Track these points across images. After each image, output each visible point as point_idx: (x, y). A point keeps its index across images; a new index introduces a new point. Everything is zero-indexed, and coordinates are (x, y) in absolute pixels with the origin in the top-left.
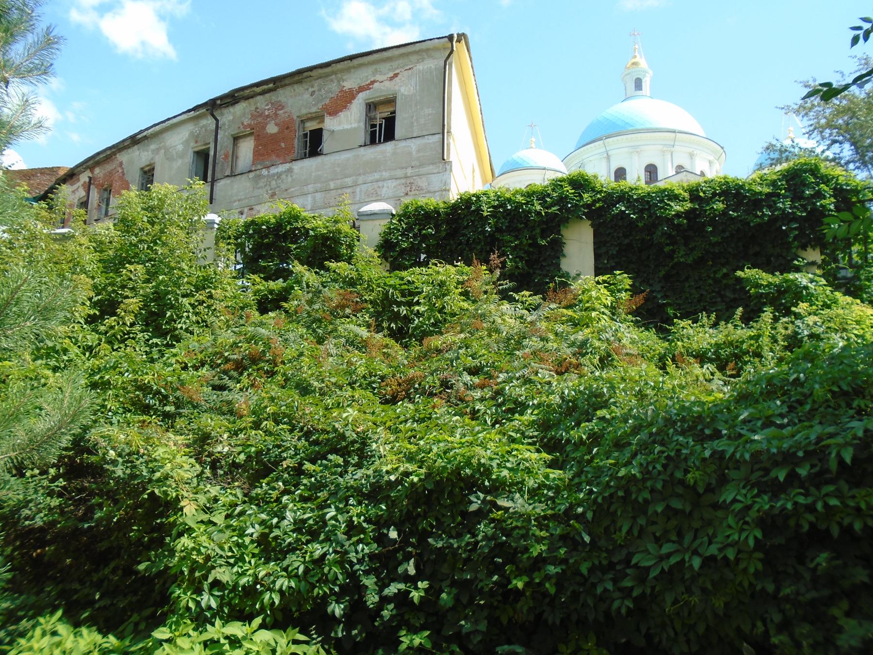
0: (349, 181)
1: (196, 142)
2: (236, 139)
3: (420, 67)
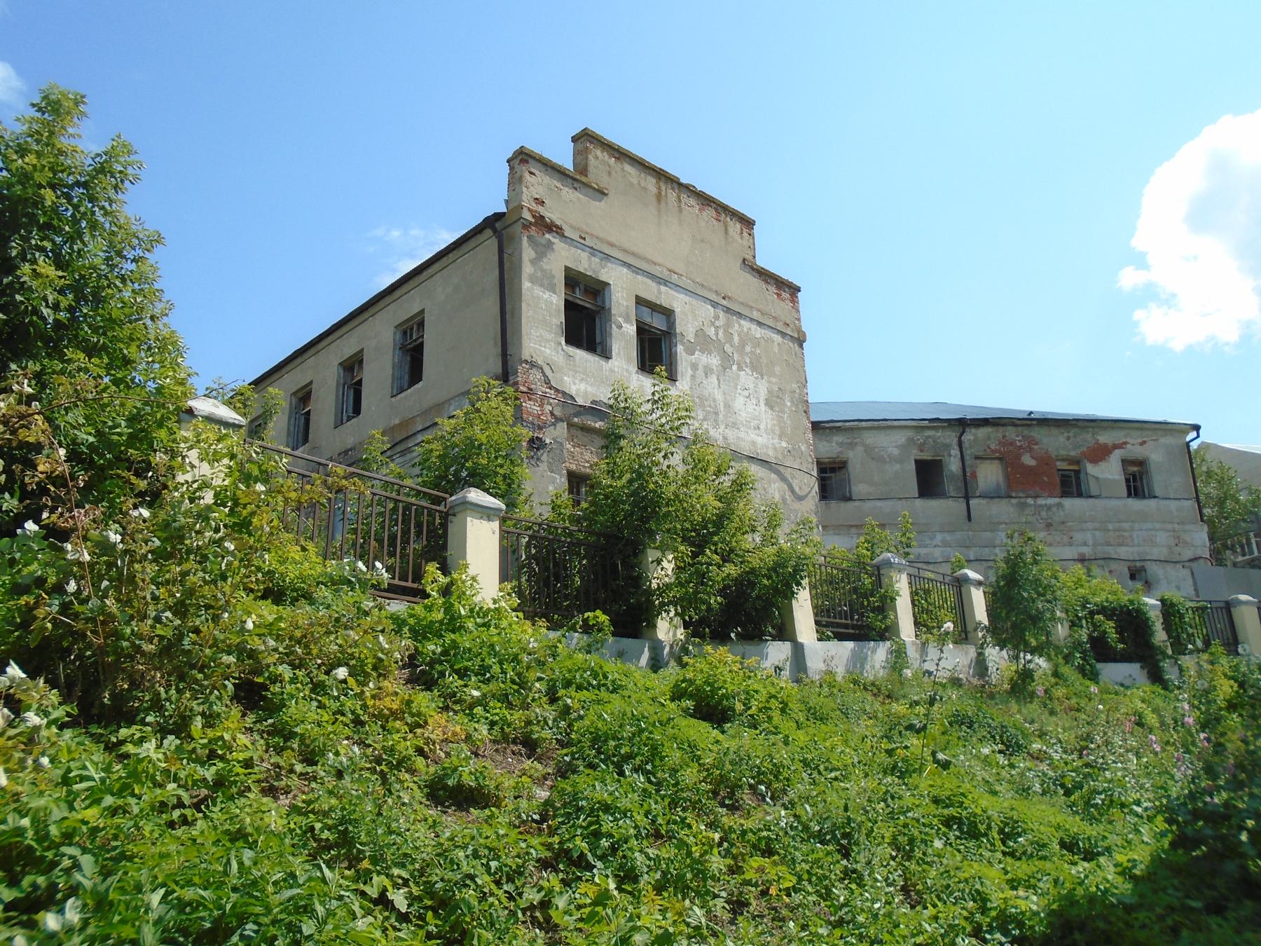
3: (1163, 440)
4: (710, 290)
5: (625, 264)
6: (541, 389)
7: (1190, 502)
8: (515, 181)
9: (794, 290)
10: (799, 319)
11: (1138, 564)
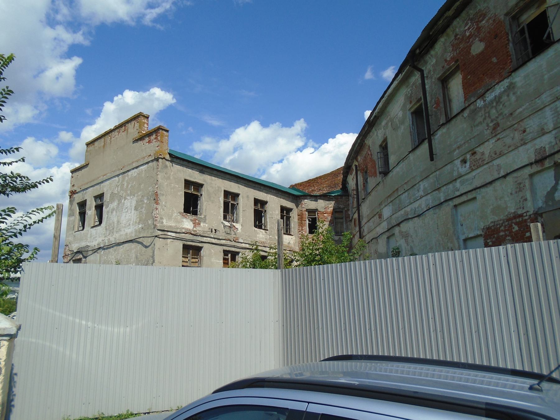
1: (411, 102)
2: (444, 81)
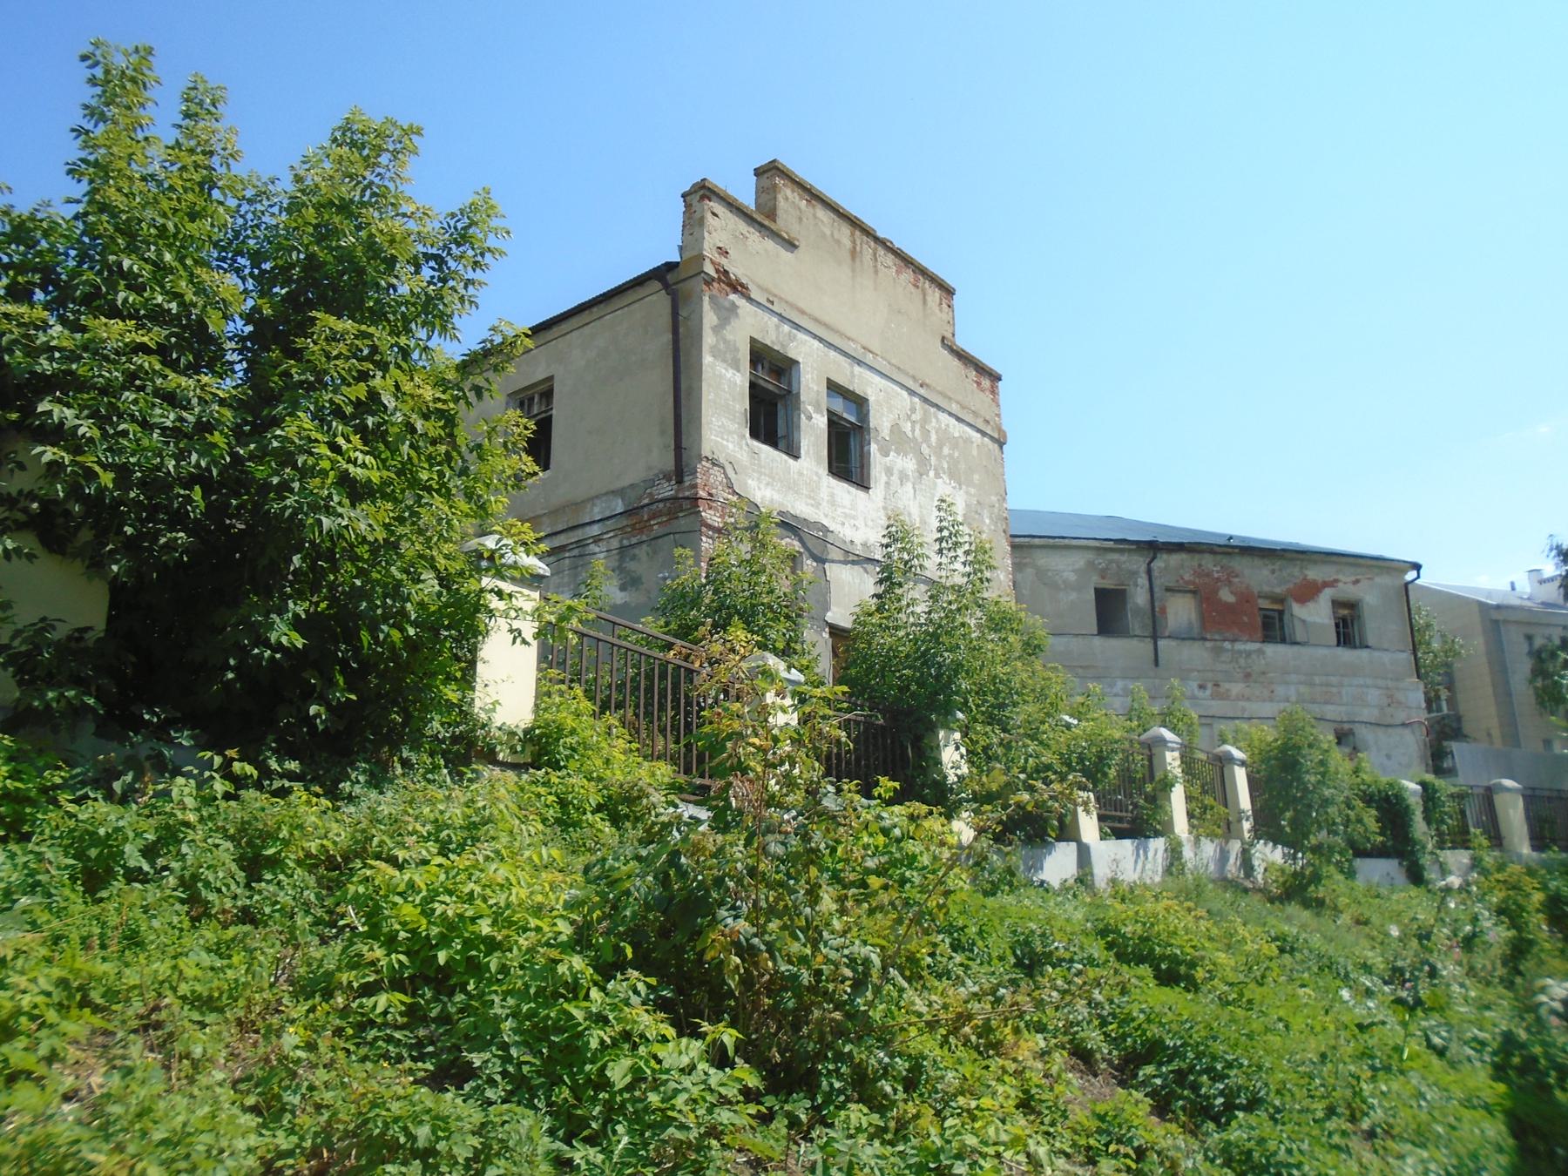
0: (1334, 680)
3: (1378, 580)
4: (907, 374)
5: (815, 337)
6: (723, 495)
7: (1404, 656)
8: (693, 223)
9: (995, 378)
10: (998, 415)
11: (1346, 726)
